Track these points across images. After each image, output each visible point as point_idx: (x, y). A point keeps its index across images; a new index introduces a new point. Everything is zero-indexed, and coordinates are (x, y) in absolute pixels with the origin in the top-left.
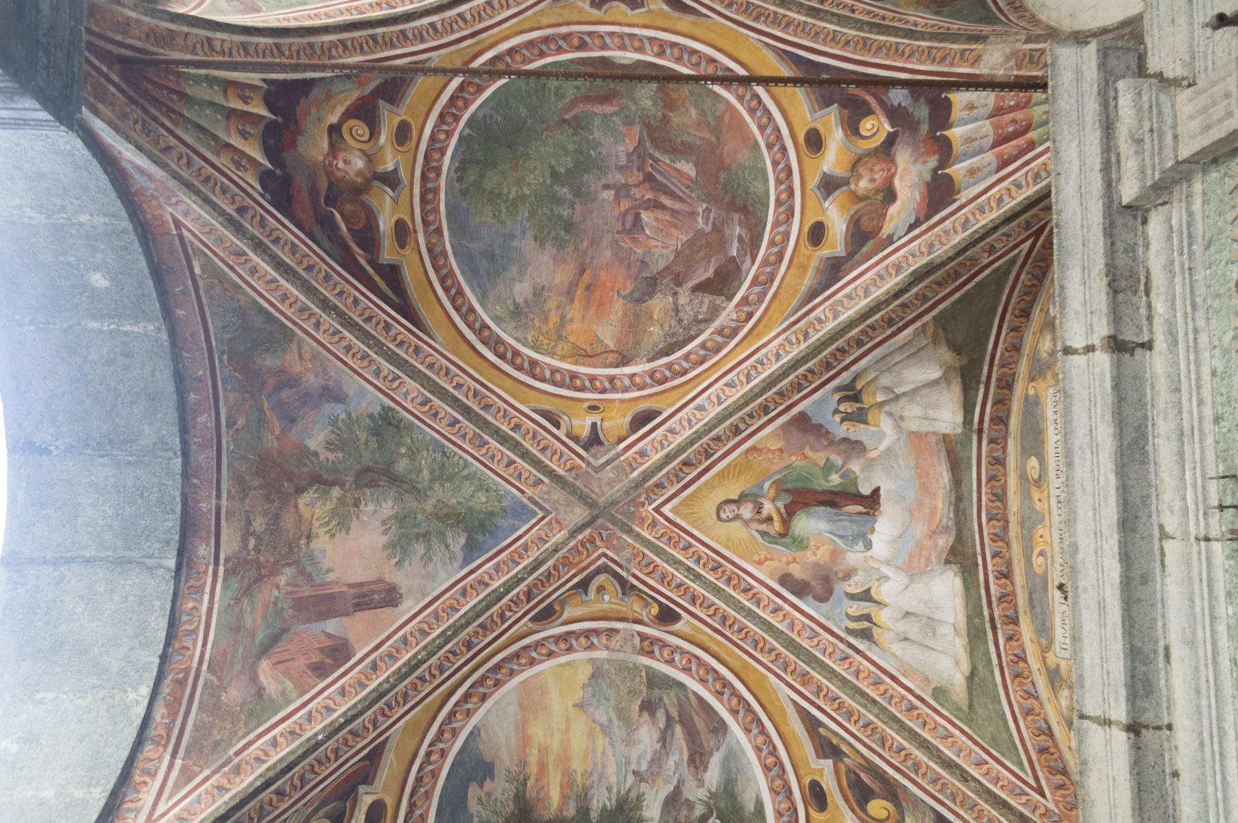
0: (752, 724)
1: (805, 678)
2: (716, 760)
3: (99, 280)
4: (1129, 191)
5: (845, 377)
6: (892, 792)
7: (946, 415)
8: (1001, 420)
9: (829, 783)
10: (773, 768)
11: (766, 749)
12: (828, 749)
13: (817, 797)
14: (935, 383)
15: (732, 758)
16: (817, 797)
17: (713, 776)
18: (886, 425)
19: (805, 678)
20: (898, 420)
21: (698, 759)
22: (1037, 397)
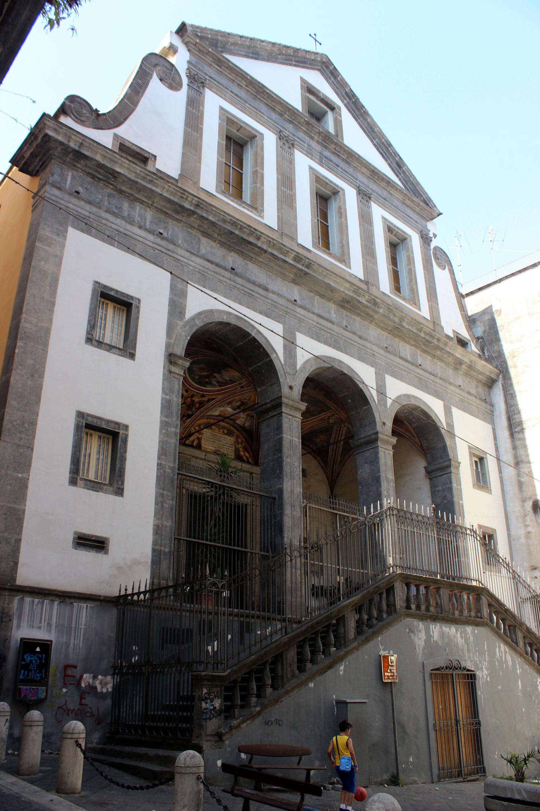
0: (218, 391)
1: (220, 401)
2: (217, 384)
3: (349, 401)
4: (254, 475)
5: (255, 418)
6: (199, 408)
7: (238, 422)
8: (233, 426)
9: (204, 399)
10: (210, 391)
11: (214, 391)
12: (209, 400)
13: (203, 396)
14: (245, 424)
15: (215, 386)
16: (203, 396)
17: (215, 383)
18: (244, 416)
19: (220, 401)
20: (243, 418)
21: (218, 382)
22: (234, 436)
